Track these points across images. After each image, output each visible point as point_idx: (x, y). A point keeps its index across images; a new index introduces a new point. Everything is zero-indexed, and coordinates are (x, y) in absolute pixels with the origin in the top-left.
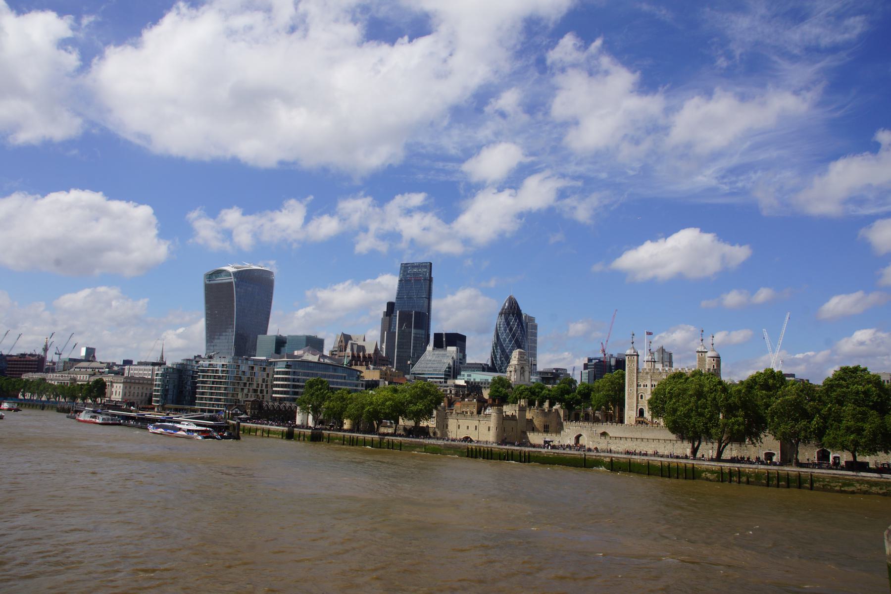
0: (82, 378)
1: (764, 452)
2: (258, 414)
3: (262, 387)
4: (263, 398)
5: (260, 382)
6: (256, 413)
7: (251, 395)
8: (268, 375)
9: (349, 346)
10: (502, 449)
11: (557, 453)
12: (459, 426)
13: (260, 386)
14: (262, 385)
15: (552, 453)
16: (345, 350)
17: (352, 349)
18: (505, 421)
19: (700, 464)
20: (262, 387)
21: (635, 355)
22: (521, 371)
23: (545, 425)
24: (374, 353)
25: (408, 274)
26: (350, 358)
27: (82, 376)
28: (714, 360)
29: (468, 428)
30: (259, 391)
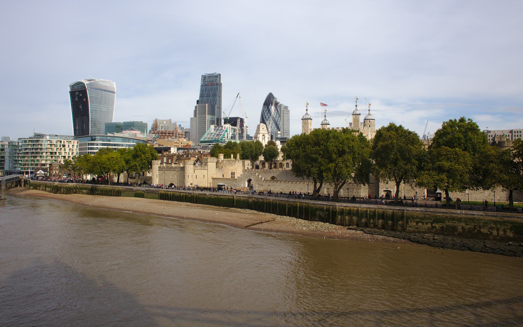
1: (382, 190)
6: (57, 173)
8: (73, 145)
11: (216, 195)
14: (69, 153)
15: (213, 195)
18: (195, 170)
19: (315, 204)
21: (308, 119)
22: (262, 138)
23: (231, 172)
25: (206, 82)
28: (370, 122)
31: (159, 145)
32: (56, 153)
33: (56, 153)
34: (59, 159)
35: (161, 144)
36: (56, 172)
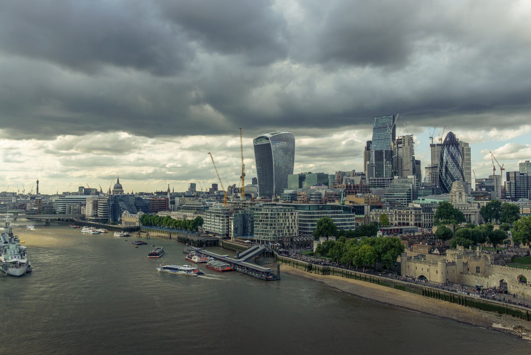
0: (189, 215)
2: (290, 245)
3: (292, 225)
4: (293, 231)
5: (290, 222)
7: (286, 230)
9: (344, 181)
10: (446, 293)
12: (416, 267)
13: (291, 224)
14: (292, 223)
16: (342, 184)
17: (346, 182)
20: (292, 225)
24: (360, 184)
26: (345, 188)
27: (189, 214)
29: (422, 269)
30: (290, 227)
31: (350, 202)
32: (282, 224)
33: (282, 224)
34: (285, 229)
35: (352, 201)
36: (288, 244)
